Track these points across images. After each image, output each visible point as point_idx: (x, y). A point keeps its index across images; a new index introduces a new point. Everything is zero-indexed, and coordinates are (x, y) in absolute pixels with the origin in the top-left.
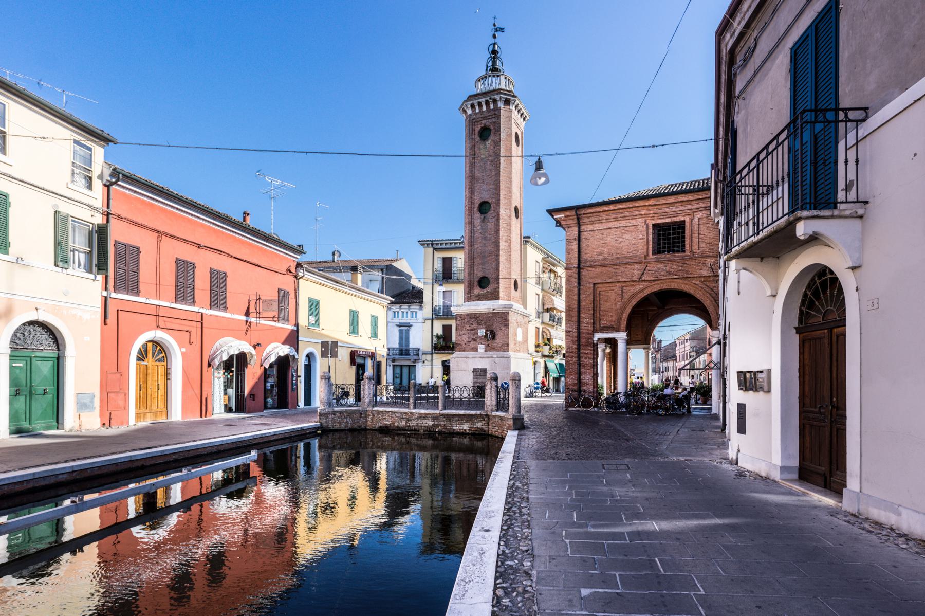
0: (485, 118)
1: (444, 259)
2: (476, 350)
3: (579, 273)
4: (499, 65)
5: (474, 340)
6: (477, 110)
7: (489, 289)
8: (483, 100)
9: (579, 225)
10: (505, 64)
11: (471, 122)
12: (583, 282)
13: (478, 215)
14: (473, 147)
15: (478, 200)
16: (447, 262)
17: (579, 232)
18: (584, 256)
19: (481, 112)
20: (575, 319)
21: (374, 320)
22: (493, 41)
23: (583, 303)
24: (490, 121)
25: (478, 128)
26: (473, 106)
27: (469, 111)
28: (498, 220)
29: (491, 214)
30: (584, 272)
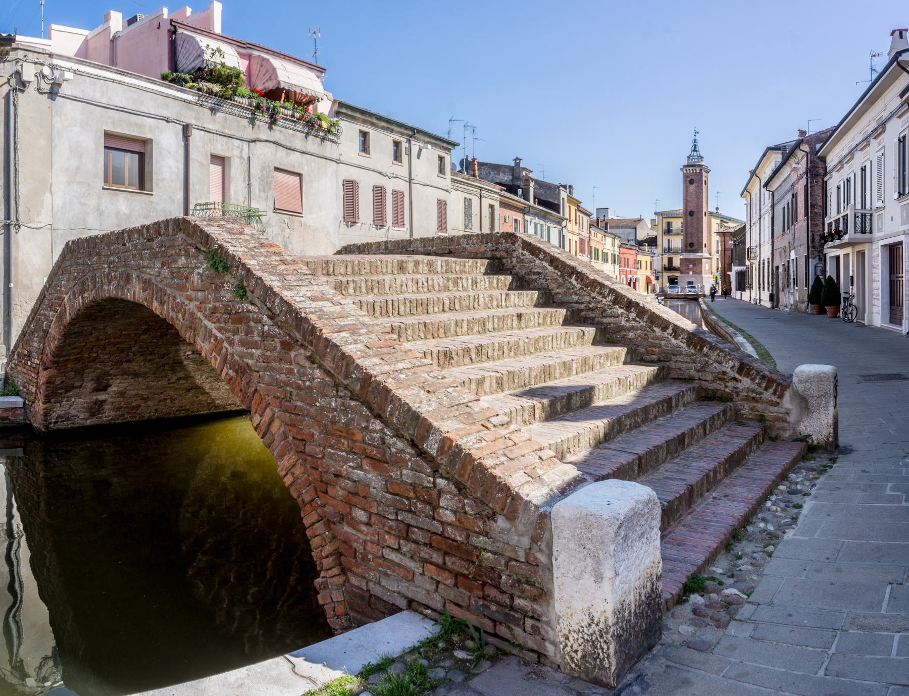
7: (694, 248)
8: (691, 169)
10: (700, 147)
11: (686, 176)
13: (689, 216)
14: (687, 187)
15: (689, 210)
16: (669, 224)
22: (694, 138)
29: (695, 216)
30: (726, 252)
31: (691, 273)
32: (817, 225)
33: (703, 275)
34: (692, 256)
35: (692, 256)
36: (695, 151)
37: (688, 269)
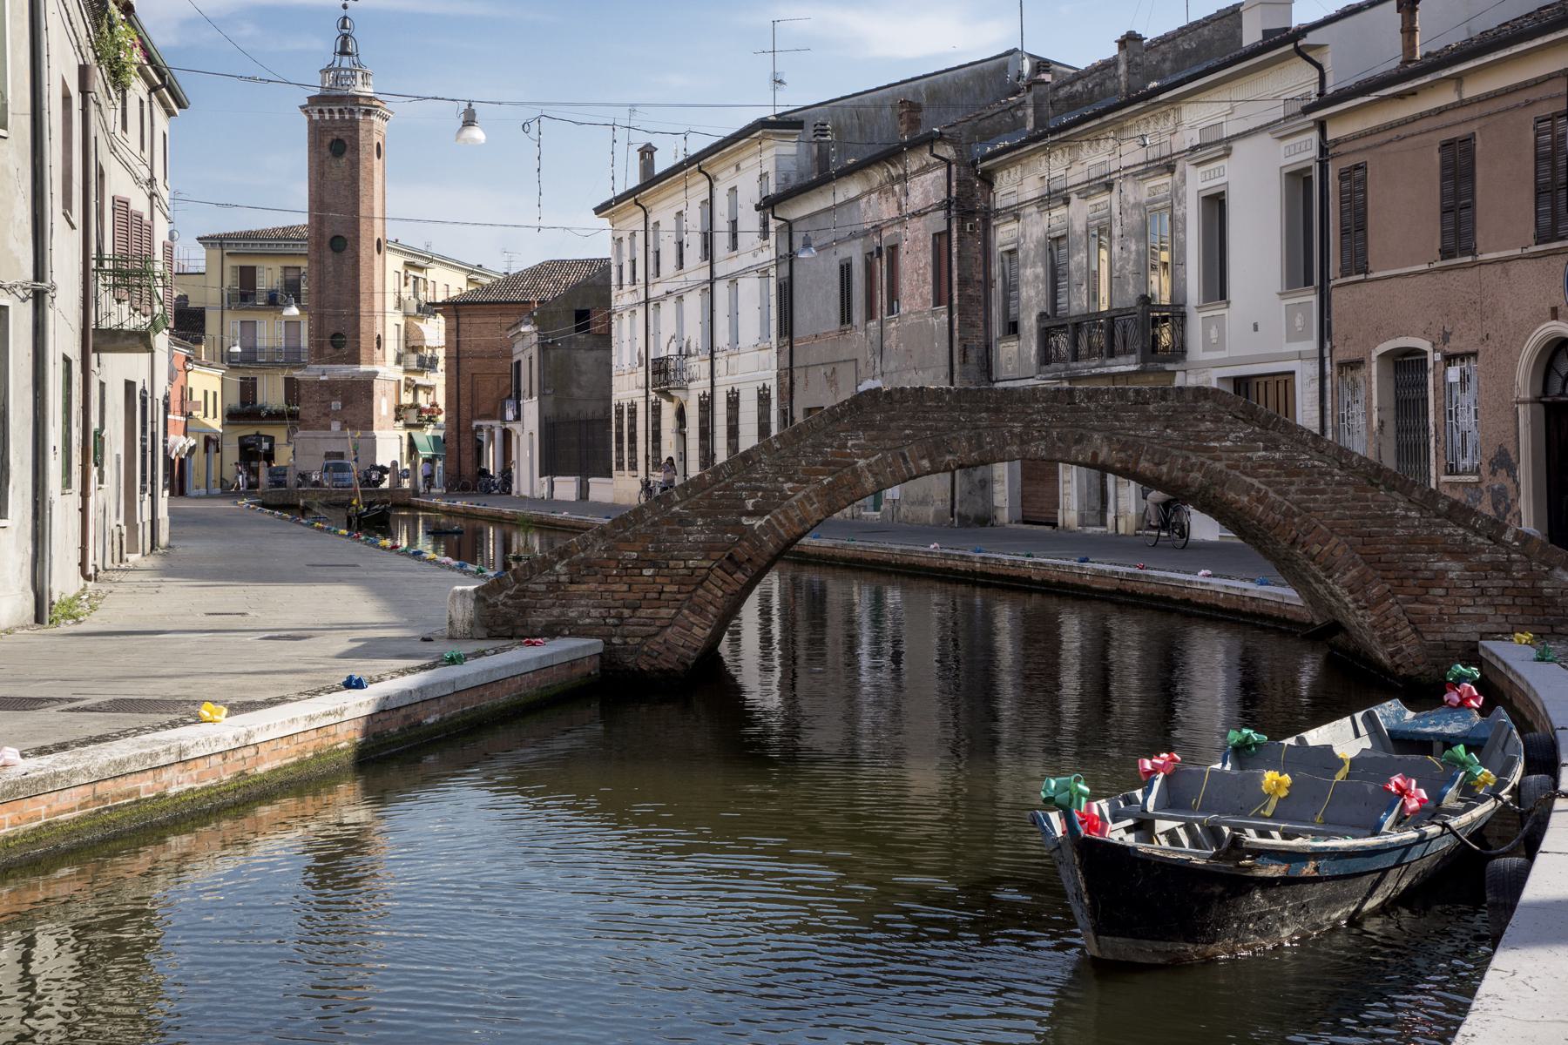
0: (335, 128)
1: (242, 268)
2: (329, 428)
3: (458, 363)
4: (351, 48)
5: (326, 415)
6: (327, 116)
7: (346, 351)
8: (335, 109)
9: (458, 317)
11: (317, 132)
12: (462, 372)
13: (329, 252)
14: (321, 163)
15: (329, 233)
16: (247, 276)
17: (458, 324)
18: (463, 347)
19: (332, 119)
20: (455, 406)
21: (215, 394)
22: (343, 13)
23: (462, 392)
24: (346, 133)
25: (328, 140)
26: (321, 111)
27: (316, 117)
28: (357, 262)
29: (348, 253)
30: (463, 363)
31: (336, 426)
32: (973, 325)
33: (376, 432)
34: (342, 371)
35: (342, 371)
36: (344, 52)
37: (328, 414)
